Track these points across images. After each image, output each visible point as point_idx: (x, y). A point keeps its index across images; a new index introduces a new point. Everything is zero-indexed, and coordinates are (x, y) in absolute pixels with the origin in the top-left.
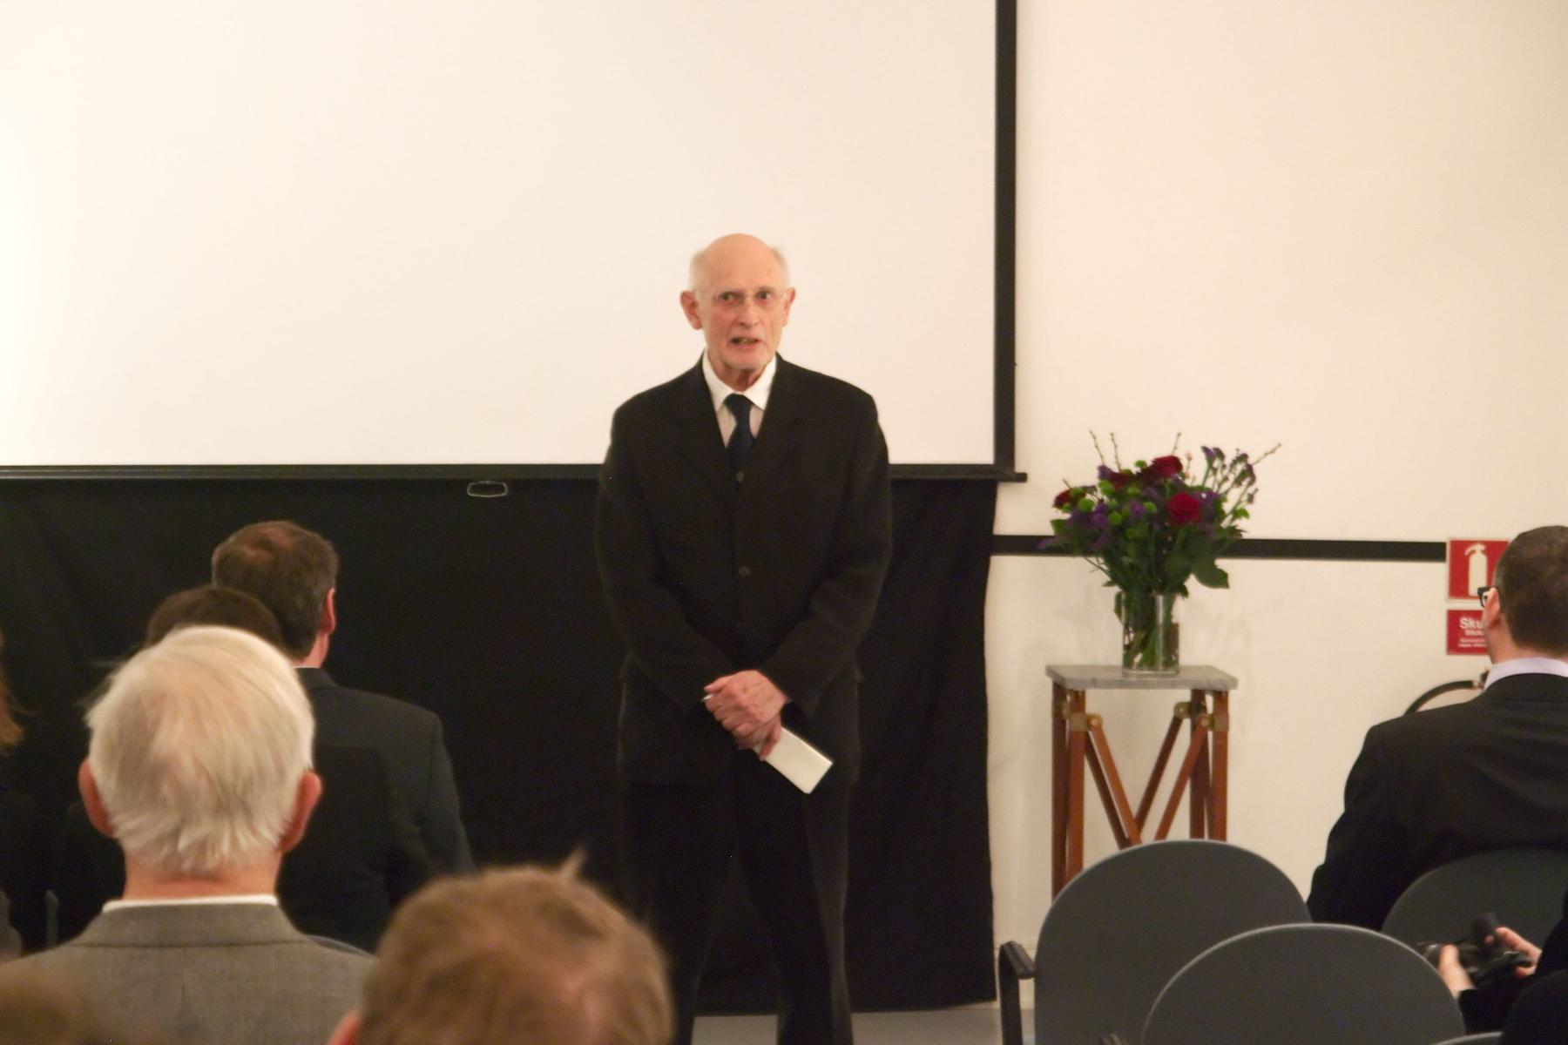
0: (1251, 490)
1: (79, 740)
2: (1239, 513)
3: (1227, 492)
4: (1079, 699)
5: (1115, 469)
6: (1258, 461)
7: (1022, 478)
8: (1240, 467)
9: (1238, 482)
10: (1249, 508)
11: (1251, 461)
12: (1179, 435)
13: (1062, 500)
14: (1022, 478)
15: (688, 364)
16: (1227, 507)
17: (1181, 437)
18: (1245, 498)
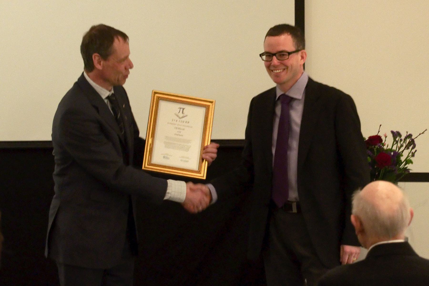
0: (413, 151)
2: (408, 161)
3: (403, 151)
8: (408, 140)
9: (407, 147)
10: (412, 159)
11: (413, 137)
12: (381, 125)
15: (79, 75)
16: (403, 159)
17: (381, 126)
18: (411, 154)
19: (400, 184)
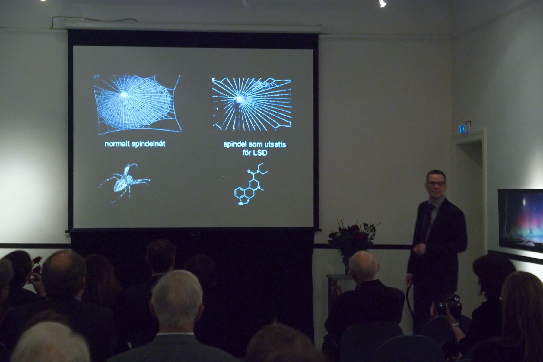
0: (374, 233)
1: (150, 295)
3: (369, 233)
4: (335, 282)
5: (342, 228)
6: (376, 226)
7: (320, 230)
8: (371, 228)
9: (371, 231)
10: (374, 237)
11: (374, 226)
12: (358, 220)
13: (330, 236)
14: (320, 230)
16: (369, 237)
17: (358, 221)
18: (373, 235)
19: (368, 250)
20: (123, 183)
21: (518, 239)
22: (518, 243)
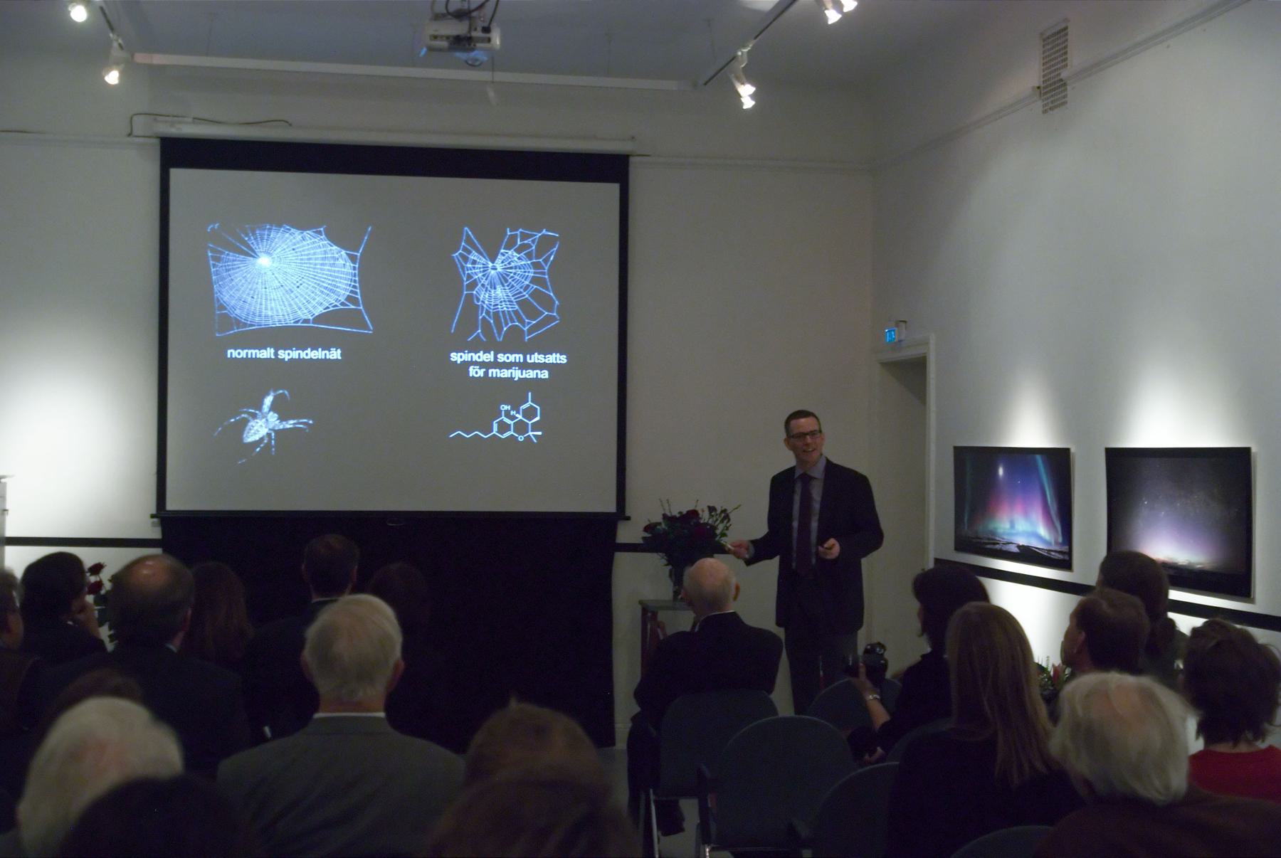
0: (728, 525)
2: (723, 535)
4: (655, 615)
5: (669, 514)
7: (628, 518)
8: (723, 515)
9: (722, 521)
10: (727, 532)
11: (728, 512)
13: (647, 529)
14: (628, 518)
16: (718, 532)
19: (715, 555)
20: (261, 426)
21: (989, 539)
22: (988, 546)
